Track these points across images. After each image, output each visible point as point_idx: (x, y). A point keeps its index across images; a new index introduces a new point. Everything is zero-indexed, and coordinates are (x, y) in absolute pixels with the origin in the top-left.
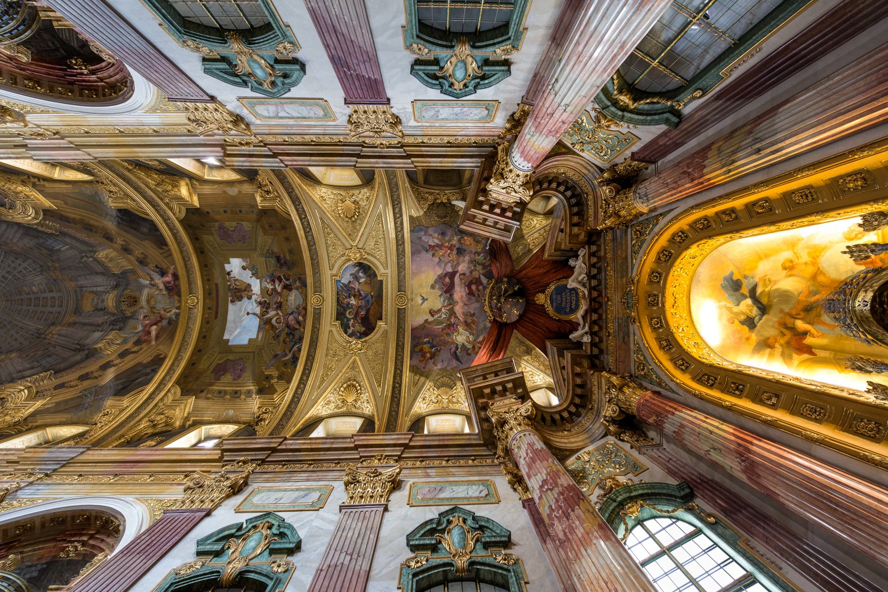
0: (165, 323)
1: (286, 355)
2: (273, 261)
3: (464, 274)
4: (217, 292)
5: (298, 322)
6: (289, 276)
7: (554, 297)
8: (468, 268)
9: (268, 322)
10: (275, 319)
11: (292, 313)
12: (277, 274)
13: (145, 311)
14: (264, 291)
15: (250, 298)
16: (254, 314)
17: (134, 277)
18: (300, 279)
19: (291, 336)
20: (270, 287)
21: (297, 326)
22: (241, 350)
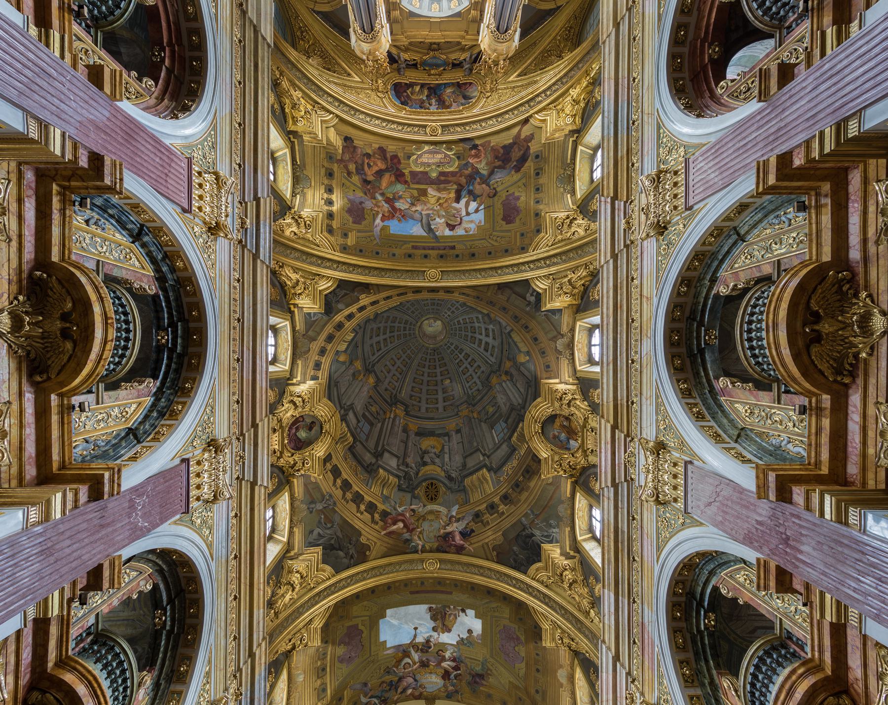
0: (407, 536)
1: (365, 696)
2: (478, 669)
4: (442, 592)
5: (405, 690)
6: (461, 681)
9: (406, 654)
11: (416, 680)
12: (462, 666)
13: (420, 510)
14: (442, 647)
16: (415, 636)
17: (461, 500)
18: (457, 692)
20: (448, 655)
21: (400, 690)
22: (373, 640)
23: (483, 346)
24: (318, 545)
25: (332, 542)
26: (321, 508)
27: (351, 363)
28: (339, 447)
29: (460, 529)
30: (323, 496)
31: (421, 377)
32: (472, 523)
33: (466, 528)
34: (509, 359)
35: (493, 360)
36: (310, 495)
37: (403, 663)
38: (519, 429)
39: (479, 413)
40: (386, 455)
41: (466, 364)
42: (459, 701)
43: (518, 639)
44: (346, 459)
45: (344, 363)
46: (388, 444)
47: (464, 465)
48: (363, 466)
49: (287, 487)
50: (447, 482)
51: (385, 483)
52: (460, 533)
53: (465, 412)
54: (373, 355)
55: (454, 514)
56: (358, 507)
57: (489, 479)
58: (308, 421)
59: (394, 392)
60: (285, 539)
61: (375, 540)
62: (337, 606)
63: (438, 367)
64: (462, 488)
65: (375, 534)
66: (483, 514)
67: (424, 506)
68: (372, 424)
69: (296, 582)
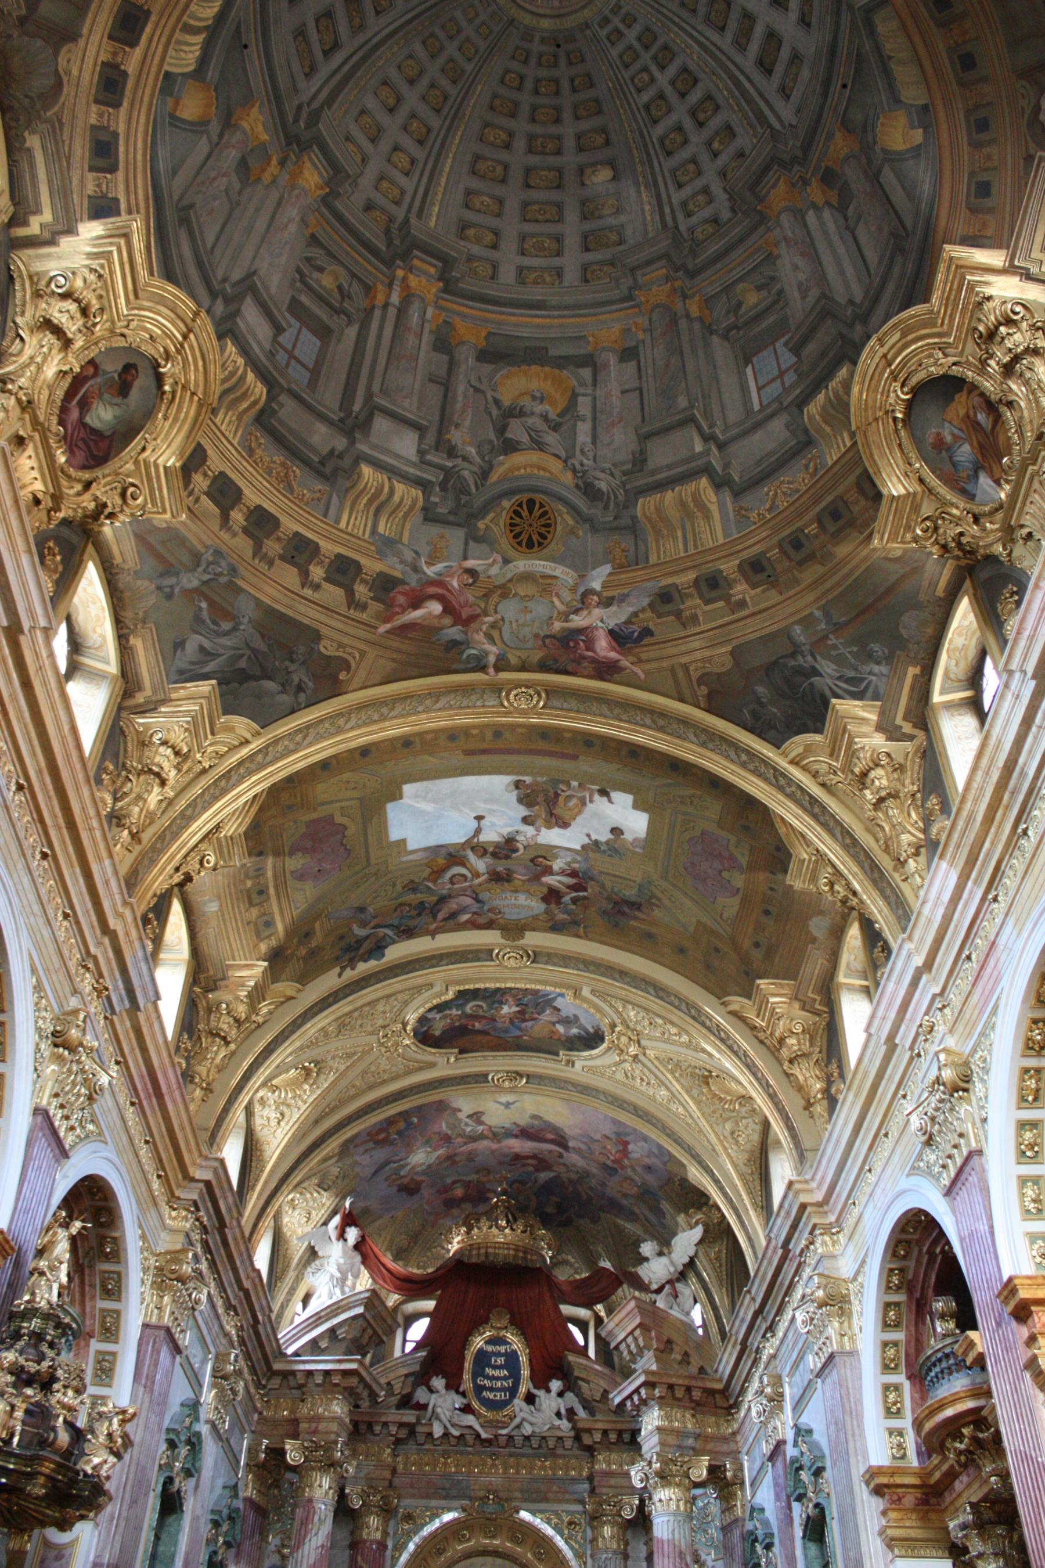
0: (454, 633)
2: (630, 893)
3: (561, 1156)
4: (551, 754)
5: (453, 915)
6: (586, 907)
7: (502, 1349)
8: (574, 1165)
10: (462, 870)
12: (592, 889)
13: (494, 571)
15: (525, 820)
16: (478, 831)
18: (576, 923)
19: (414, 912)
20: (557, 865)
21: (441, 916)
22: (372, 839)
23: (754, 48)
24: (206, 677)
25: (243, 664)
26: (195, 583)
27: (228, 122)
28: (225, 420)
29: (612, 624)
30: (197, 558)
31: (504, 156)
32: (649, 614)
33: (628, 622)
34: (846, 125)
35: (787, 112)
36: (158, 556)
37: (449, 875)
38: (834, 384)
39: (708, 302)
40: (381, 424)
41: (680, 114)
42: (578, 936)
43: (732, 858)
44: (251, 452)
45: (199, 126)
46: (384, 391)
47: (640, 460)
48: (306, 463)
49: (90, 549)
50: (580, 502)
51: (379, 506)
52: (611, 632)
53: (659, 293)
54: (311, 71)
55: (597, 585)
56: (305, 574)
57: (714, 508)
58: (112, 367)
59: (400, 213)
60: (113, 667)
61: (363, 646)
62: (274, 791)
63: (567, 116)
64: (625, 521)
65: (361, 633)
66: (683, 597)
67: (506, 561)
68: (324, 333)
69: (166, 765)
